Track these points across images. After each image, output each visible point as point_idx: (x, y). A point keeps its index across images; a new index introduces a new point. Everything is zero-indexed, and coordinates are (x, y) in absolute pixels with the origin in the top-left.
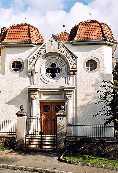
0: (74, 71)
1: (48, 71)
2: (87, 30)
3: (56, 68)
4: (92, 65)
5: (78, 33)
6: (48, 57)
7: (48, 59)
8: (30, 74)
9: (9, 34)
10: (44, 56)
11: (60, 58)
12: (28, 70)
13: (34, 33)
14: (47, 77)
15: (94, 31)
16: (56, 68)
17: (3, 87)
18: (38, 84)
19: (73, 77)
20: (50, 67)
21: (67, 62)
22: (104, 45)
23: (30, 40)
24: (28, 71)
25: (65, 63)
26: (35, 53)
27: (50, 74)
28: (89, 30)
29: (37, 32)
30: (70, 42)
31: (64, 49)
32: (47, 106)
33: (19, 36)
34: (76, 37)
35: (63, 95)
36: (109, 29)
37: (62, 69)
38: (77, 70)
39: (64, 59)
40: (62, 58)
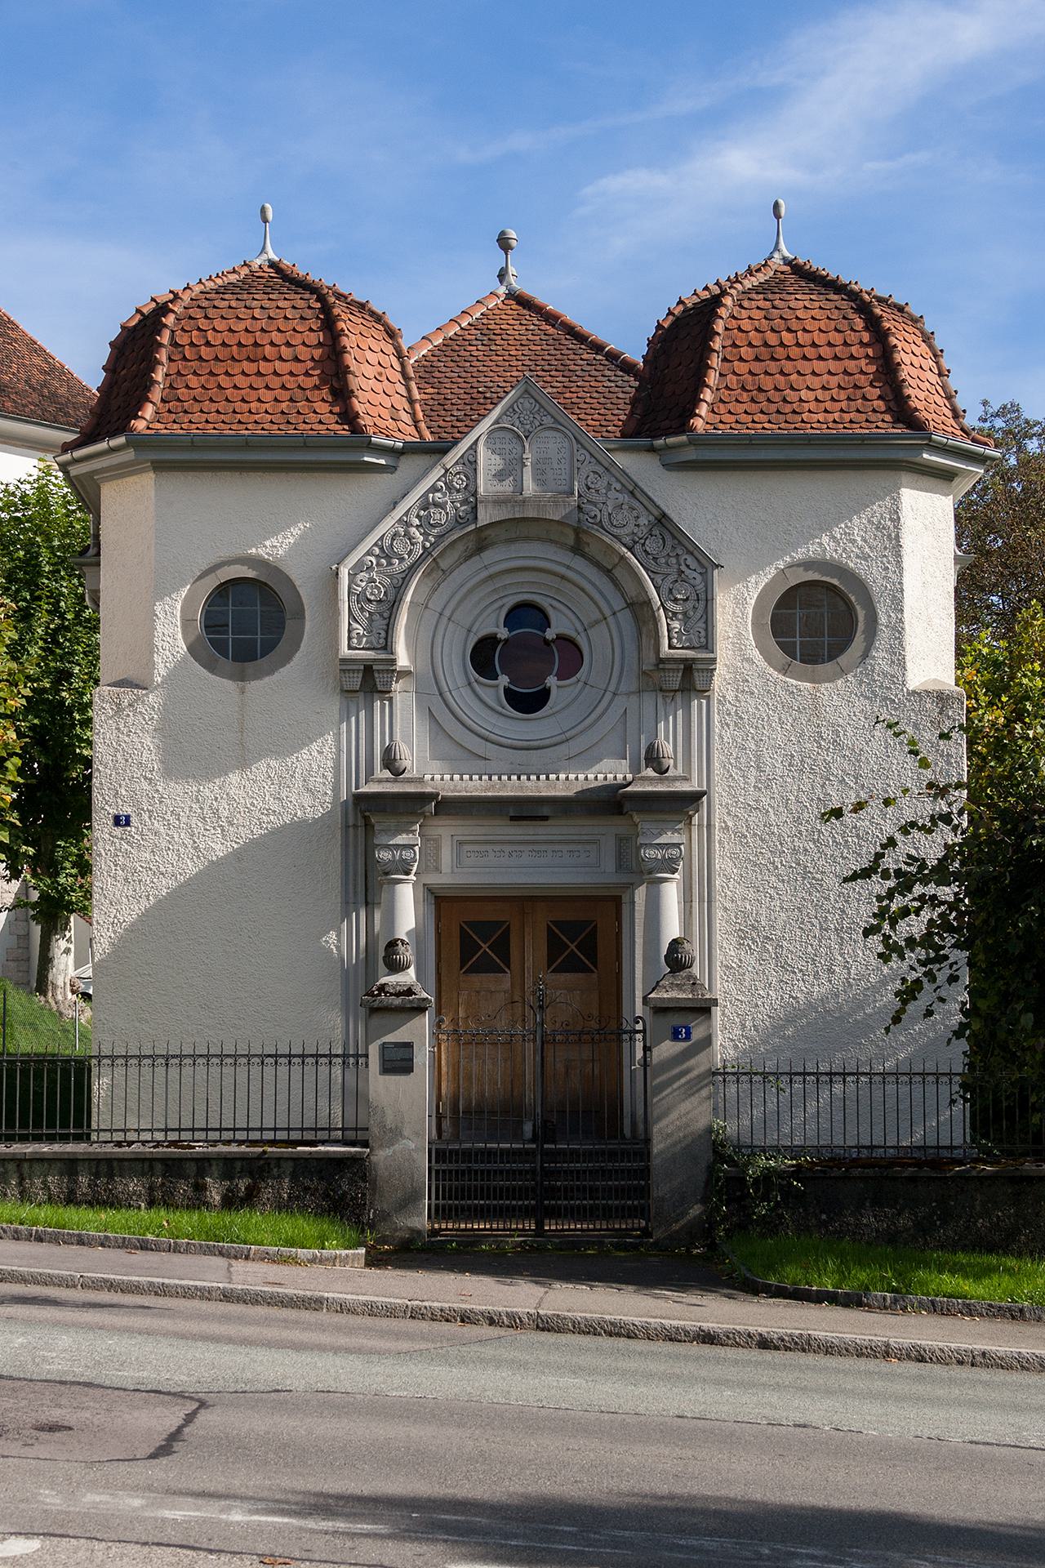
0: (688, 667)
1: (484, 656)
2: (780, 352)
3: (550, 634)
4: (823, 621)
5: (712, 378)
6: (489, 556)
7: (492, 570)
8: (356, 681)
9: (170, 359)
10: (461, 547)
11: (579, 563)
12: (345, 651)
13: (369, 355)
14: (482, 703)
15: (832, 365)
16: (550, 634)
17: (145, 785)
18: (425, 767)
19: (680, 712)
20: (503, 633)
21: (631, 591)
22: (905, 477)
23: (349, 417)
24: (344, 661)
25: (618, 603)
26: (386, 526)
27: (504, 680)
28: (795, 352)
29: (390, 349)
30: (660, 442)
31: (612, 494)
32: (484, 928)
33: (258, 382)
34: (703, 410)
35: (609, 847)
36: (931, 347)
37: (598, 646)
38: (715, 660)
39: (608, 572)
40: (598, 565)
